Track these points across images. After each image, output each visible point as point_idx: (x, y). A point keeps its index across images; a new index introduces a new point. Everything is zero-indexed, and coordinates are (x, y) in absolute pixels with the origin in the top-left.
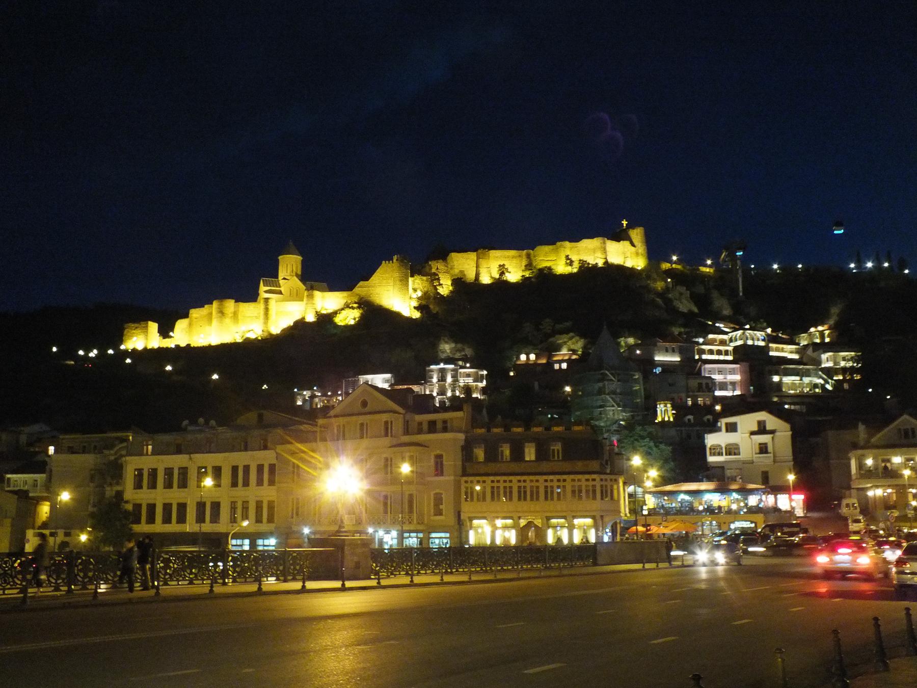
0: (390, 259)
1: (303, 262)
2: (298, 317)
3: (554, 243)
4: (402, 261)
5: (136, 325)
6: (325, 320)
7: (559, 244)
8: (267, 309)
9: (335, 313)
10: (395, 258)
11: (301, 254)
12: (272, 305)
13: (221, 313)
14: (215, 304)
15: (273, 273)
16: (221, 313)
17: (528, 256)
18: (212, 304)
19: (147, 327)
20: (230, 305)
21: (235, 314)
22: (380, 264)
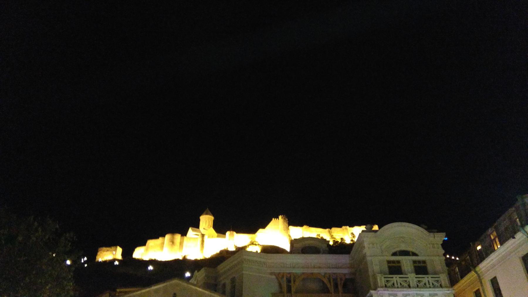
0: (277, 217)
1: (214, 222)
2: (222, 248)
3: (341, 227)
4: (284, 219)
5: (108, 249)
6: (240, 250)
7: (344, 227)
8: (203, 241)
9: (246, 247)
10: (280, 217)
11: (214, 215)
12: (206, 238)
13: (172, 242)
14: (168, 237)
15: (196, 225)
16: (172, 242)
17: (329, 232)
18: (164, 236)
19: (116, 250)
20: (178, 237)
21: (181, 244)
22: (271, 220)
